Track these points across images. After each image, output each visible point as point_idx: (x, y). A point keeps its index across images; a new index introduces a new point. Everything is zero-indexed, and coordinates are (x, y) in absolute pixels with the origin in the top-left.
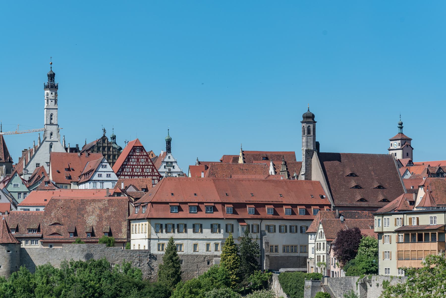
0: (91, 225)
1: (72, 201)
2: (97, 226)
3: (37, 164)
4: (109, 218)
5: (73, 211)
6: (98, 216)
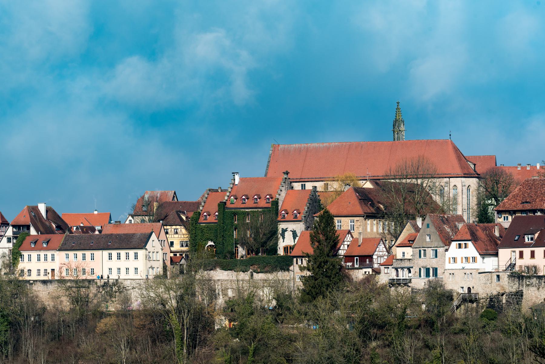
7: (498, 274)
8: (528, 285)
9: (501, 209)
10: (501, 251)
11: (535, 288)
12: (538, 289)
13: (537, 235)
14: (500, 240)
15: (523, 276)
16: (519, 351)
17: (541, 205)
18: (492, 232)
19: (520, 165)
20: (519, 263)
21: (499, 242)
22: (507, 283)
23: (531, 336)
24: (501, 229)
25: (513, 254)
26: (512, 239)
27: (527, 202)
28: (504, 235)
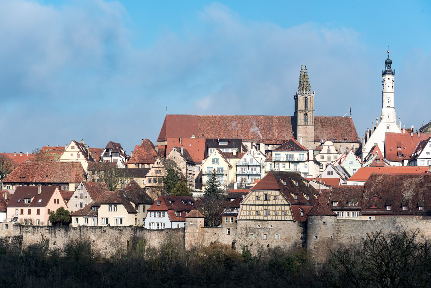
0: (407, 199)
1: (390, 176)
2: (413, 200)
3: (375, 144)
4: (424, 193)
5: (391, 186)
6: (414, 190)
7: (6, 224)
8: (26, 232)
9: (6, 181)
10: (9, 209)
11: (31, 234)
12: (33, 235)
13: (32, 199)
14: (8, 202)
15: (23, 226)
16: (22, 275)
17: (32, 180)
18: (2, 196)
19: (15, 152)
20: (21, 217)
21: (7, 203)
22: (12, 230)
23: (29, 265)
24: (9, 194)
25: (17, 211)
26: (16, 201)
27: (23, 177)
28: (10, 199)
